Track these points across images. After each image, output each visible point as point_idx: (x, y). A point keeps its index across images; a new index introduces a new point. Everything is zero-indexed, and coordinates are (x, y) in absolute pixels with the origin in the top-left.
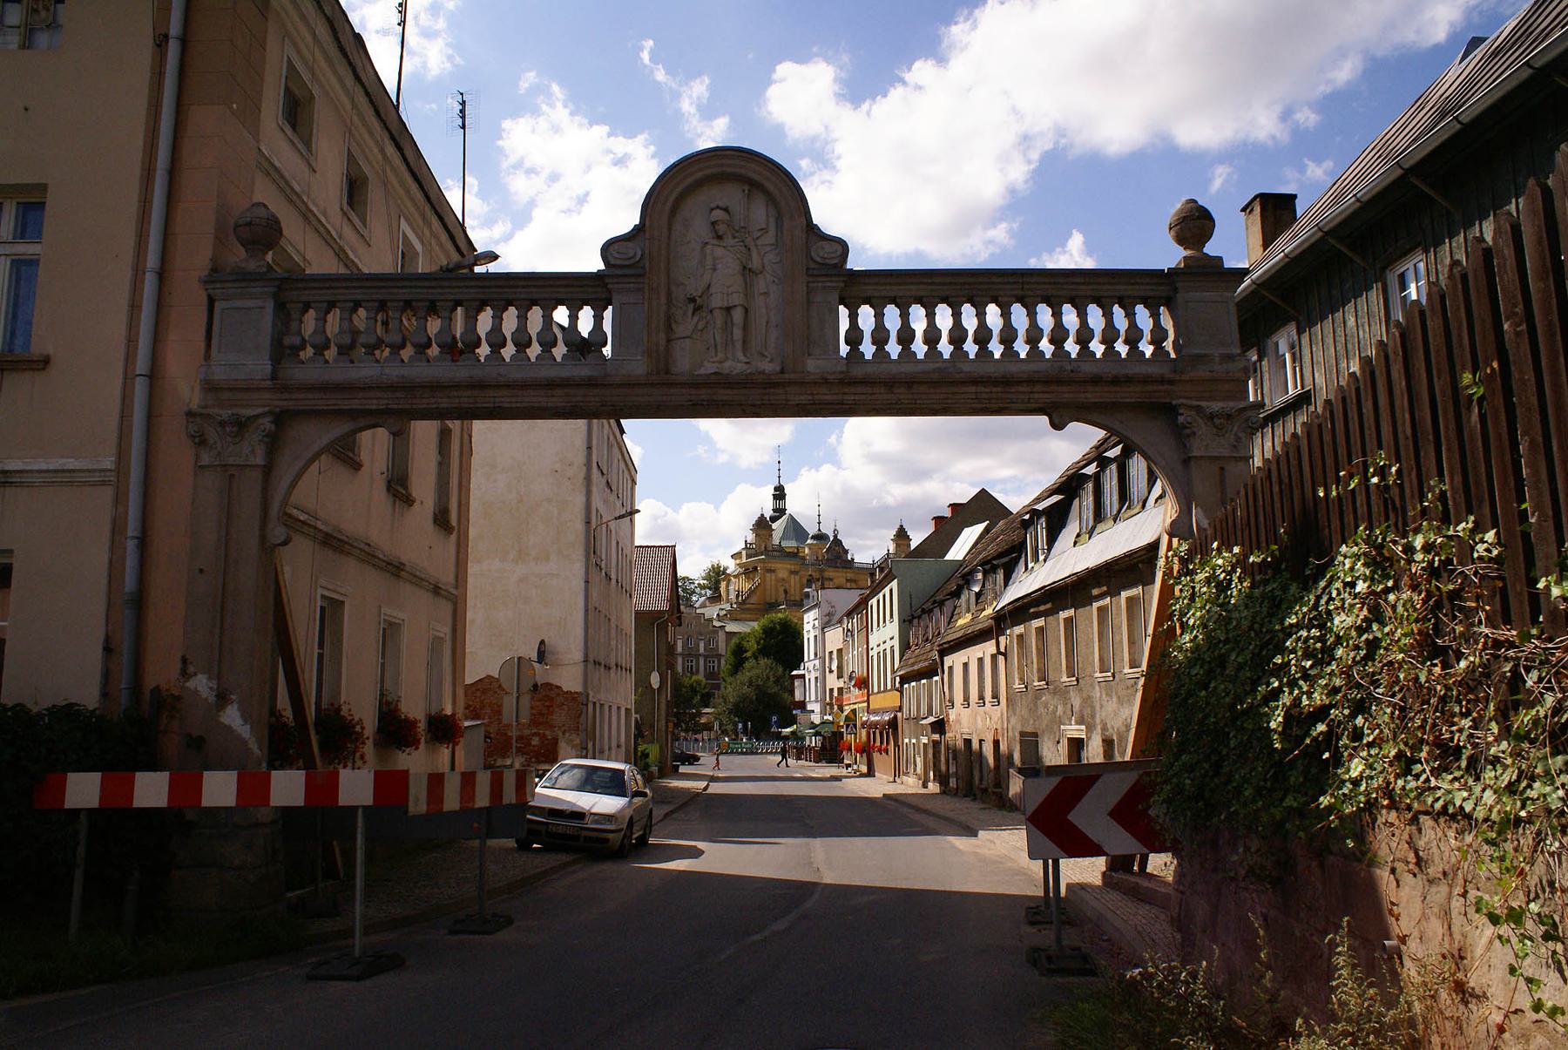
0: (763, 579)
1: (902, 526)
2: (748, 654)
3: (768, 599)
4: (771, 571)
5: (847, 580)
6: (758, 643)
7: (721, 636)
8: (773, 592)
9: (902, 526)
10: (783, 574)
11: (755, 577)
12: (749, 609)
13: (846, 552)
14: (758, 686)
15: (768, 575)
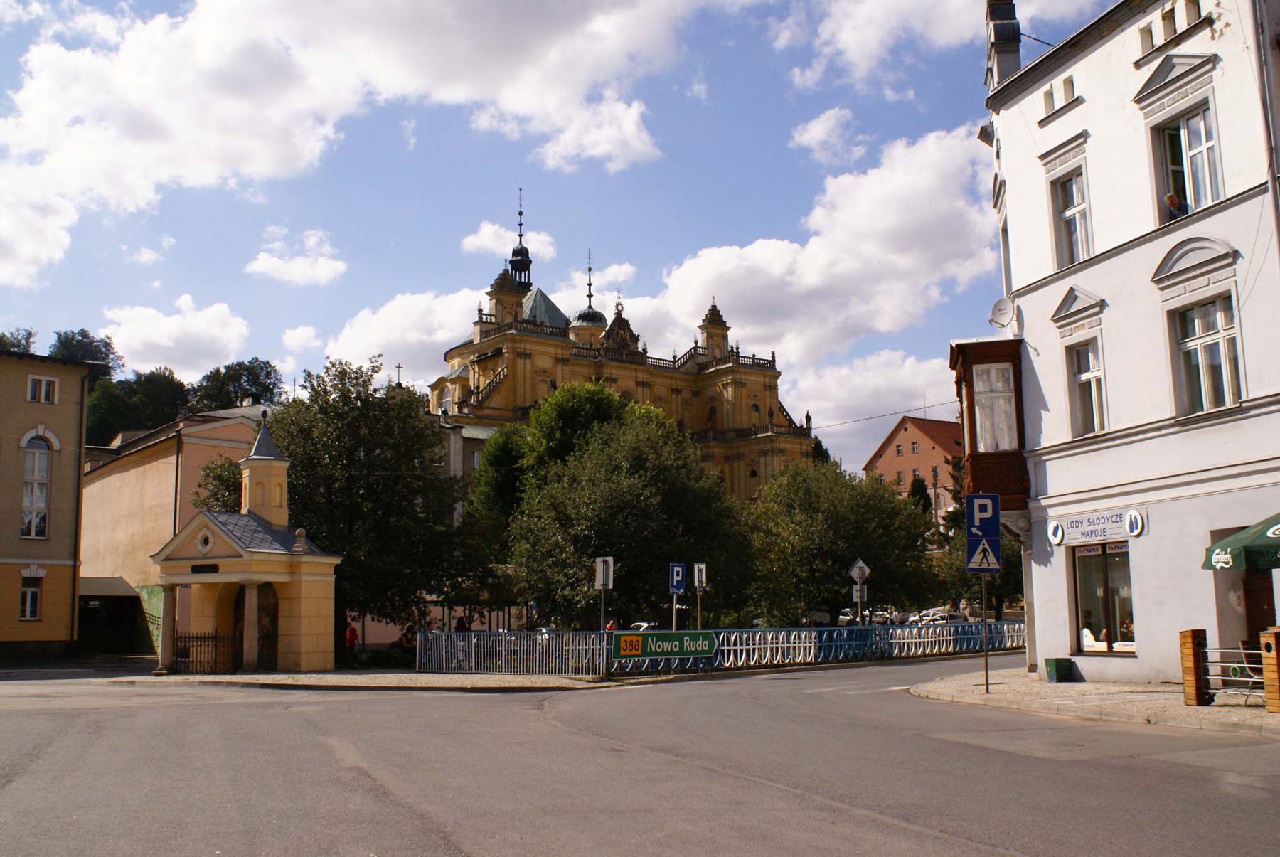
0: (512, 366)
1: (714, 307)
2: (524, 462)
3: (520, 402)
4: (526, 356)
5: (638, 384)
6: (550, 437)
7: (455, 445)
8: (529, 382)
9: (714, 307)
10: (544, 362)
11: (497, 366)
12: (488, 417)
13: (636, 339)
14: (662, 469)
15: (520, 361)
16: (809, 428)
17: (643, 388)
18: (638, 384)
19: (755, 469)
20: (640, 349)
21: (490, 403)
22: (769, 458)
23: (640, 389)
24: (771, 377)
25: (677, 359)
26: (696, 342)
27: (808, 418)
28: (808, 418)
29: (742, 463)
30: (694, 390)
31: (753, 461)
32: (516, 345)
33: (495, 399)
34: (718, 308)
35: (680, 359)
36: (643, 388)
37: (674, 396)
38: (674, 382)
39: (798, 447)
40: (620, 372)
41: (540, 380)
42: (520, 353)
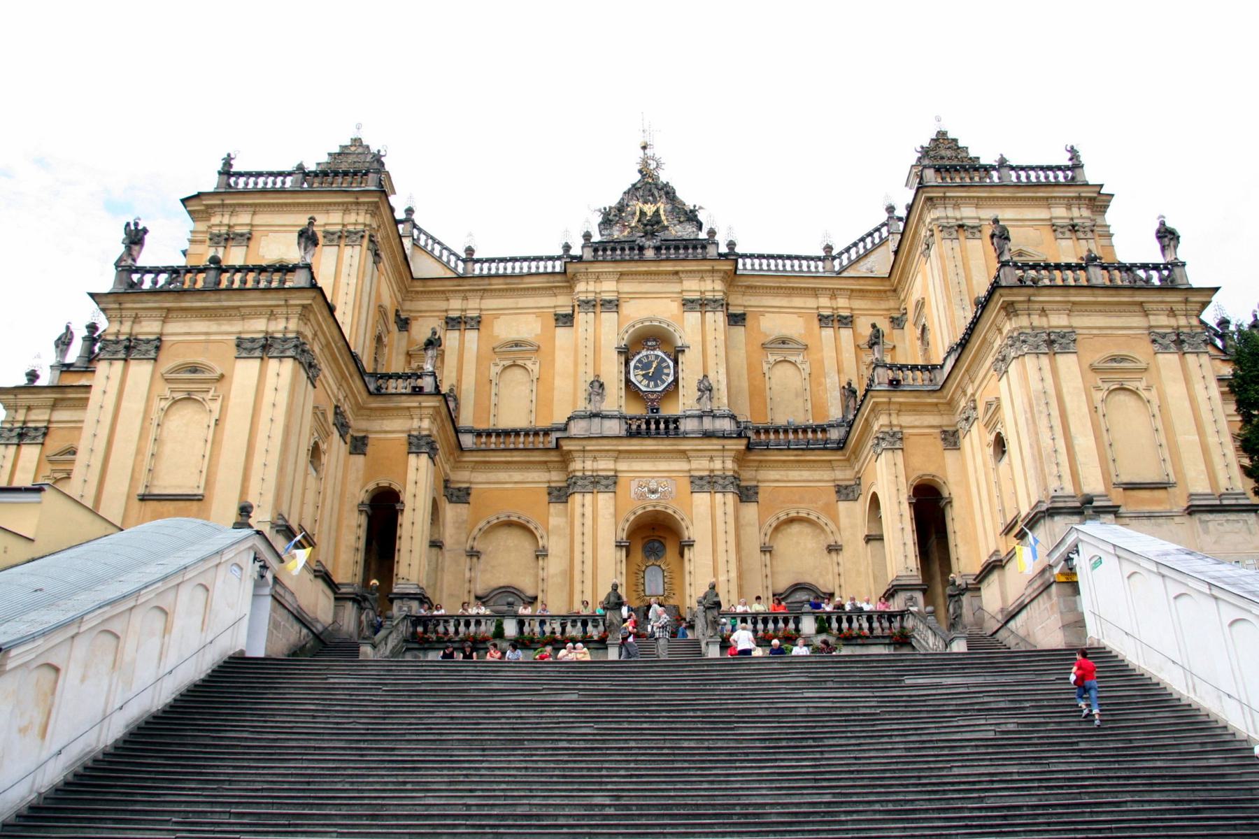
13: (691, 217)
16: (1176, 265)
17: (703, 313)
18: (688, 304)
19: (998, 431)
20: (703, 235)
22: (1013, 368)
23: (693, 318)
24: (1069, 203)
25: (834, 253)
26: (891, 209)
27: (1167, 236)
28: (1167, 236)
29: (974, 429)
30: (896, 315)
31: (989, 404)
32: (215, 220)
34: (951, 135)
35: (841, 254)
36: (703, 313)
37: (828, 333)
38: (824, 301)
39: (1138, 321)
40: (627, 287)
42: (219, 236)
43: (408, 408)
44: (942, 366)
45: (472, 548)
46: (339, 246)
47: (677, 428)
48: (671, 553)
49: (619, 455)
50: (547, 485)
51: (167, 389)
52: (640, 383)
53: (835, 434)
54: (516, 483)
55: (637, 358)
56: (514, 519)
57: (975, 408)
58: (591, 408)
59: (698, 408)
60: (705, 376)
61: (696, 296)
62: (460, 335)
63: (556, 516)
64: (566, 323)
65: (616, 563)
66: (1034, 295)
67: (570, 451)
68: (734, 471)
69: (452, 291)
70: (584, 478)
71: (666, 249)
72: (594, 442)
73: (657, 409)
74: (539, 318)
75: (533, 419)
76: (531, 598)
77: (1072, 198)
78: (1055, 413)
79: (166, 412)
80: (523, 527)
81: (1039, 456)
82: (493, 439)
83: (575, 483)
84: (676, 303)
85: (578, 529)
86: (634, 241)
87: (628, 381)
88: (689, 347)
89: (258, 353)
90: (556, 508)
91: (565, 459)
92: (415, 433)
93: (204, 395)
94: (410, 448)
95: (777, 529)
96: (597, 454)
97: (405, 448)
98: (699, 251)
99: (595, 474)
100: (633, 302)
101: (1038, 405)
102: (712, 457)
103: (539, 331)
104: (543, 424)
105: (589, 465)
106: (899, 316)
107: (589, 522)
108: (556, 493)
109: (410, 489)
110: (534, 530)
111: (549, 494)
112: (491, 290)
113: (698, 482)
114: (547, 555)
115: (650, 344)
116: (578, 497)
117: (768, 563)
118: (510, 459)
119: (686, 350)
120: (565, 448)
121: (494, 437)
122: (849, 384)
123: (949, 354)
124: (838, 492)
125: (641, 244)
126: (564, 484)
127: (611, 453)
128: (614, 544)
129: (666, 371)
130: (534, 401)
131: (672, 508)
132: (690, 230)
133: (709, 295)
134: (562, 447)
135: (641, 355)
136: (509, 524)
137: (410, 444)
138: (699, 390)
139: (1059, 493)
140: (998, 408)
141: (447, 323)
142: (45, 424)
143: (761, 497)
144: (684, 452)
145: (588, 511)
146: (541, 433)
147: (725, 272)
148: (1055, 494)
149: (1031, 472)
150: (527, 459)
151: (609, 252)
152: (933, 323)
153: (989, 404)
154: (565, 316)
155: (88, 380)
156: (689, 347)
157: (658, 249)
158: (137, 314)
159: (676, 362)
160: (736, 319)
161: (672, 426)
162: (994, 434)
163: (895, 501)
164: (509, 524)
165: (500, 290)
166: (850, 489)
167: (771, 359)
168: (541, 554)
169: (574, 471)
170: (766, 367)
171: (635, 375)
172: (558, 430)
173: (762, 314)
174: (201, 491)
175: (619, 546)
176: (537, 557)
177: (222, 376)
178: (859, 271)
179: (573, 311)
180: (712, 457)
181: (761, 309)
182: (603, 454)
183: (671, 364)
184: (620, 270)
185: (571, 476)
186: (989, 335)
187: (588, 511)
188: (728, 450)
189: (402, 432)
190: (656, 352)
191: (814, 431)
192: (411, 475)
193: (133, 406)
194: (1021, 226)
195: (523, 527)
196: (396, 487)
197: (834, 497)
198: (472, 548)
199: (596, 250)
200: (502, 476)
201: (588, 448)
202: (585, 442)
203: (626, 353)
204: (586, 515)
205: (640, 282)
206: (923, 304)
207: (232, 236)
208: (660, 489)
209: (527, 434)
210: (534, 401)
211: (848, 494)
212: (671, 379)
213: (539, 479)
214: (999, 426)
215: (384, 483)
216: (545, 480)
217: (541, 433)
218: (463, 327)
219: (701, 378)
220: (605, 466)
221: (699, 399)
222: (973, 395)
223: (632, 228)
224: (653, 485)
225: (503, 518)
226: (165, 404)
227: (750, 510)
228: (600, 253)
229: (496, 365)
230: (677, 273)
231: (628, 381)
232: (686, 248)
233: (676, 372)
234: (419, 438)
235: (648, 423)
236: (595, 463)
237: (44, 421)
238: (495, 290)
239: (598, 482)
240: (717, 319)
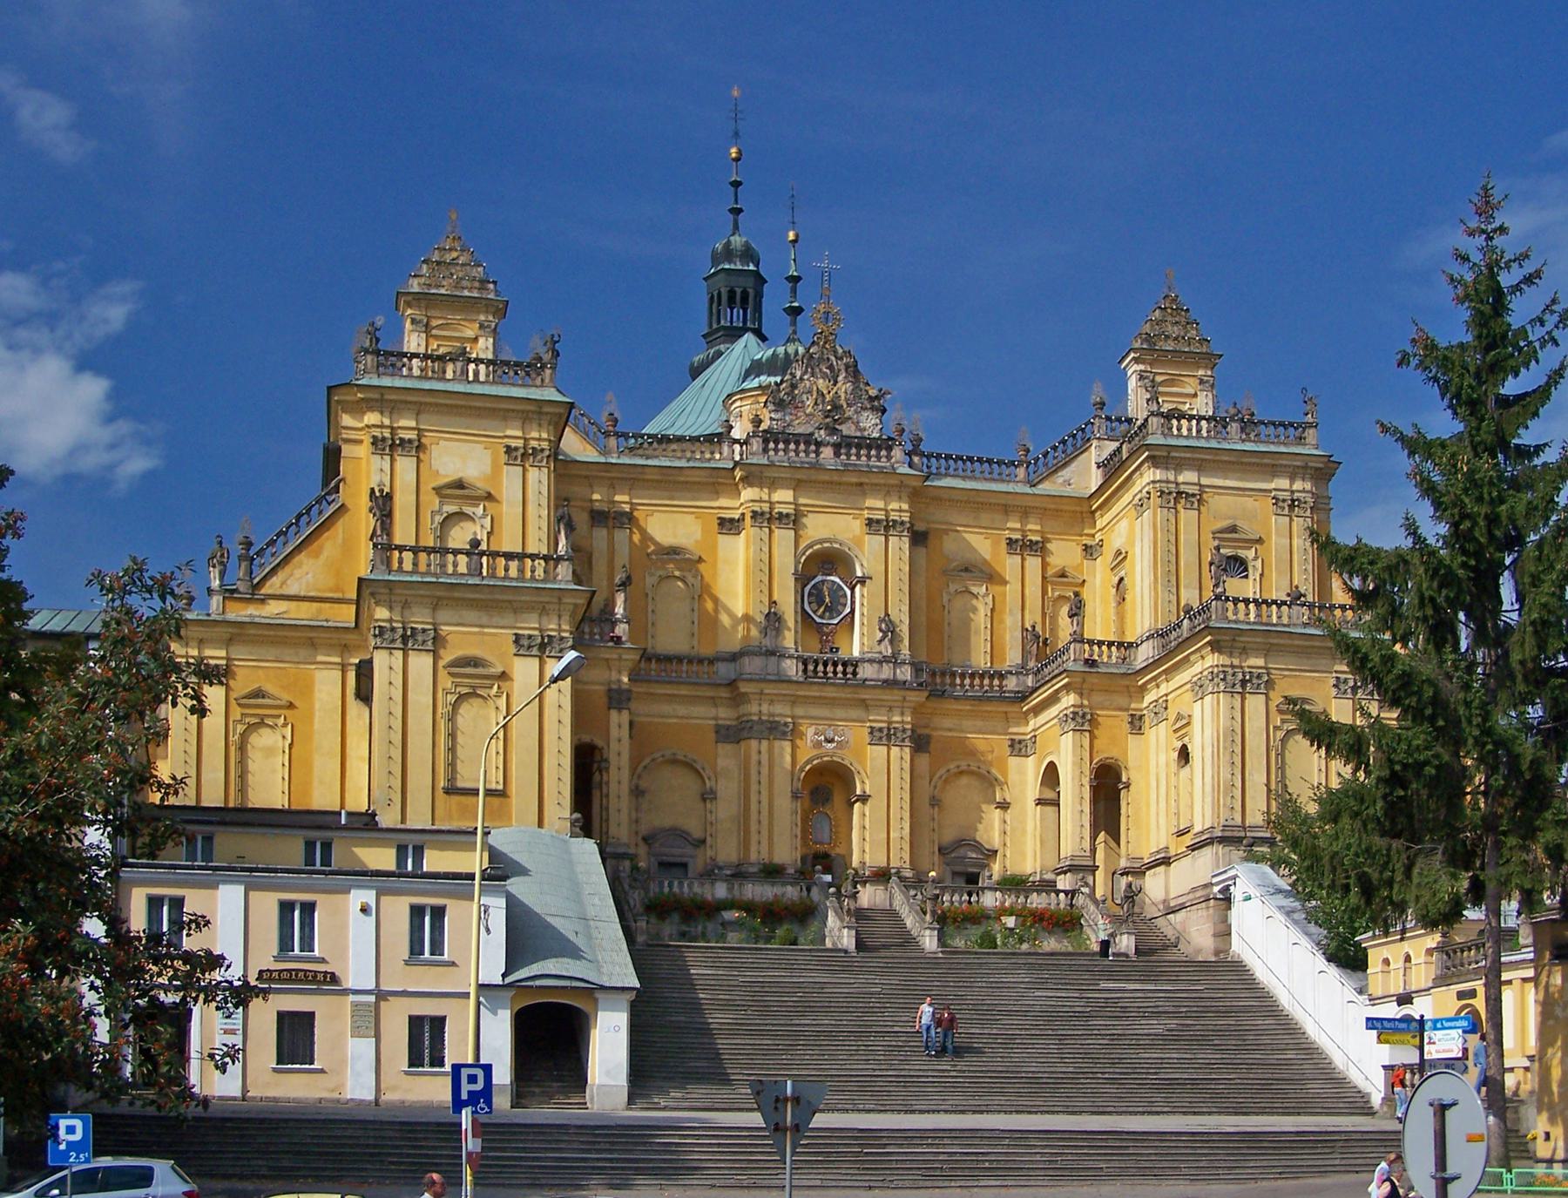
21: (283, 583)
22: (1208, 699)
33: (298, 573)
41: (450, 517)
43: (607, 660)
44: (1137, 646)
45: (637, 787)
46: (523, 466)
47: (855, 673)
48: (838, 800)
49: (795, 701)
50: (713, 722)
51: (450, 683)
52: (815, 612)
53: (1011, 683)
54: (682, 717)
55: (813, 582)
56: (680, 757)
57: (1166, 708)
58: (767, 642)
59: (877, 649)
60: (887, 614)
61: (880, 516)
62: (608, 534)
63: (726, 758)
64: (731, 529)
65: (792, 815)
66: (1239, 636)
67: (746, 693)
68: (913, 725)
69: (596, 477)
70: (761, 721)
71: (846, 446)
72: (772, 685)
73: (837, 649)
74: (700, 521)
75: (695, 643)
76: (694, 840)
77: (1298, 467)
78: (1238, 750)
79: (455, 706)
80: (690, 766)
81: (1216, 788)
82: (653, 665)
83: (751, 728)
84: (858, 522)
85: (754, 777)
86: (812, 434)
87: (803, 608)
88: (871, 578)
89: (535, 651)
90: (725, 749)
91: (738, 699)
92: (614, 687)
93: (487, 690)
94: (610, 703)
95: (946, 781)
96: (774, 697)
97: (605, 700)
98: (883, 453)
99: (771, 719)
100: (810, 515)
101: (1225, 741)
102: (891, 708)
103: (698, 536)
104: (706, 651)
105: (765, 708)
106: (1093, 543)
107: (765, 771)
108: (723, 732)
109: (614, 746)
110: (701, 771)
111: (717, 732)
112: (644, 480)
113: (877, 734)
114: (716, 798)
115: (826, 567)
116: (754, 743)
117: (936, 816)
118: (676, 692)
119: (868, 581)
120: (743, 690)
121: (653, 662)
122: (1034, 627)
123: (1148, 638)
124: (1011, 746)
125: (819, 439)
126: (734, 723)
127: (788, 698)
128: (790, 794)
129: (842, 600)
130: (696, 623)
131: (847, 758)
132: (873, 422)
133: (894, 516)
134: (738, 688)
135: (816, 580)
136: (674, 762)
137: (610, 698)
138: (881, 630)
139: (1230, 823)
140: (1188, 724)
141: (593, 518)
142: (224, 662)
143: (932, 746)
144: (864, 700)
145: (765, 758)
146: (706, 663)
147: (914, 488)
148: (1227, 823)
149: (1208, 799)
150: (693, 693)
151: (781, 446)
152: (1134, 585)
153: (1179, 717)
154: (732, 520)
155: (256, 609)
156: (871, 578)
157: (837, 447)
158: (406, 600)
159: (852, 589)
160: (919, 539)
161: (850, 669)
162: (1179, 744)
163: (1077, 783)
164: (674, 762)
165: (652, 481)
166: (1023, 744)
167: (952, 588)
168: (708, 796)
169: (751, 715)
170: (945, 598)
171: (810, 603)
172: (724, 660)
173: (946, 532)
174: (500, 787)
175: (795, 796)
176: (704, 800)
177: (504, 673)
178: (1055, 483)
179: (743, 520)
180: (891, 708)
181: (944, 527)
182: (781, 698)
183: (849, 593)
184: (799, 477)
185: (745, 719)
186: (1192, 658)
187: (765, 758)
188: (910, 701)
189: (602, 684)
190: (832, 578)
191: (992, 677)
192: (614, 732)
193: (421, 698)
194: (1240, 495)
195: (690, 766)
196: (599, 742)
197: (1008, 750)
198: (637, 787)
199: (766, 441)
200: (666, 708)
201: (766, 691)
202: (763, 685)
203: (802, 579)
204: (763, 762)
205: (819, 492)
206: (1125, 557)
207: (398, 442)
208: (836, 738)
209: (690, 661)
210: (696, 623)
211: (1020, 750)
212: (848, 610)
213: (706, 714)
214: (1186, 739)
215: (586, 738)
216: (711, 716)
217: (706, 663)
218: (611, 523)
219: (882, 616)
220: (782, 711)
221: (880, 642)
222: (1166, 695)
223: (807, 415)
224: (830, 734)
225: (668, 753)
226: (452, 698)
227: (924, 760)
228: (772, 445)
229: (652, 575)
230: (861, 484)
231: (803, 608)
232: (869, 448)
233: (853, 603)
234: (620, 691)
235: (825, 665)
236: (771, 707)
237: (222, 658)
238: (648, 480)
239: (775, 728)
240: (900, 545)
